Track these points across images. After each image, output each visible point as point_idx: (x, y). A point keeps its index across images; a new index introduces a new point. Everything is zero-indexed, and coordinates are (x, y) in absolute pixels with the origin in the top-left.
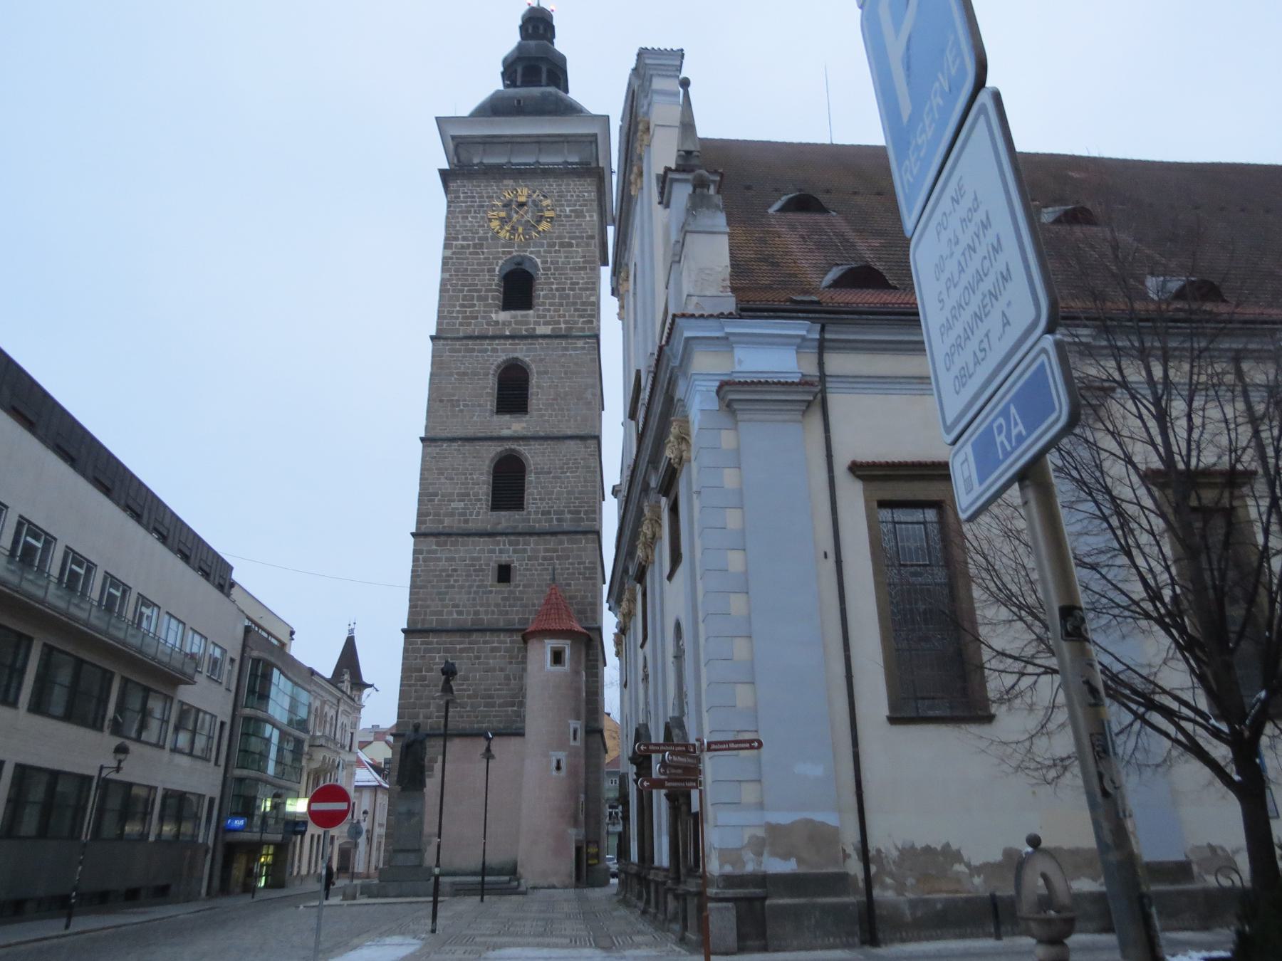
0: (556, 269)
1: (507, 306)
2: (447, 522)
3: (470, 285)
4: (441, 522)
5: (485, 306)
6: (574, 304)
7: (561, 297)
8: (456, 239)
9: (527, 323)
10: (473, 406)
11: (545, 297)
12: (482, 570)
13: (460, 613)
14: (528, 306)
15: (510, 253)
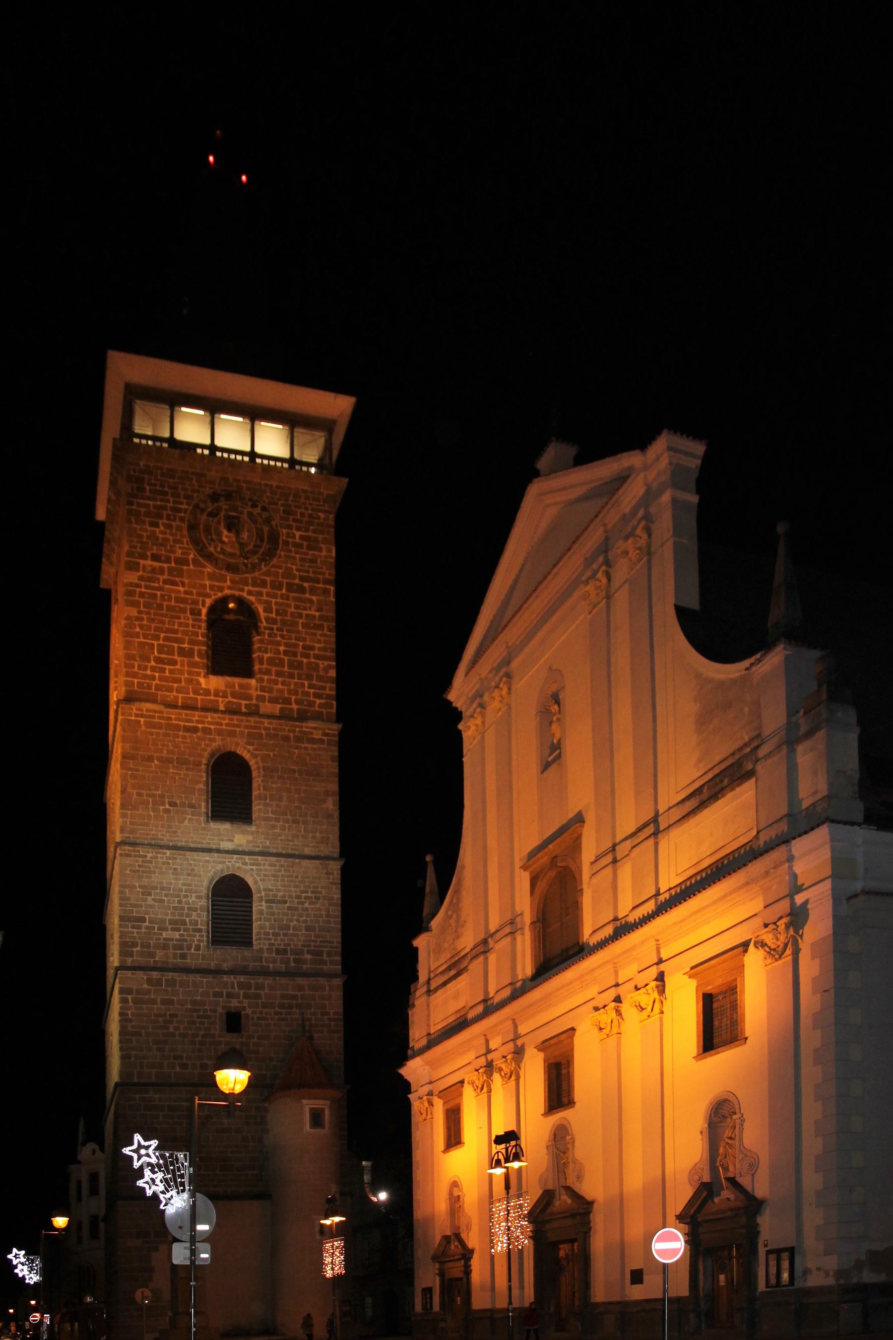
0: (284, 623)
1: (215, 669)
2: (159, 955)
3: (168, 631)
4: (153, 955)
5: (192, 665)
6: (309, 677)
7: (291, 665)
8: (144, 557)
9: (248, 697)
10: (183, 805)
11: (271, 661)
12: (209, 1017)
13: (184, 1066)
14: (248, 673)
15: (221, 589)
